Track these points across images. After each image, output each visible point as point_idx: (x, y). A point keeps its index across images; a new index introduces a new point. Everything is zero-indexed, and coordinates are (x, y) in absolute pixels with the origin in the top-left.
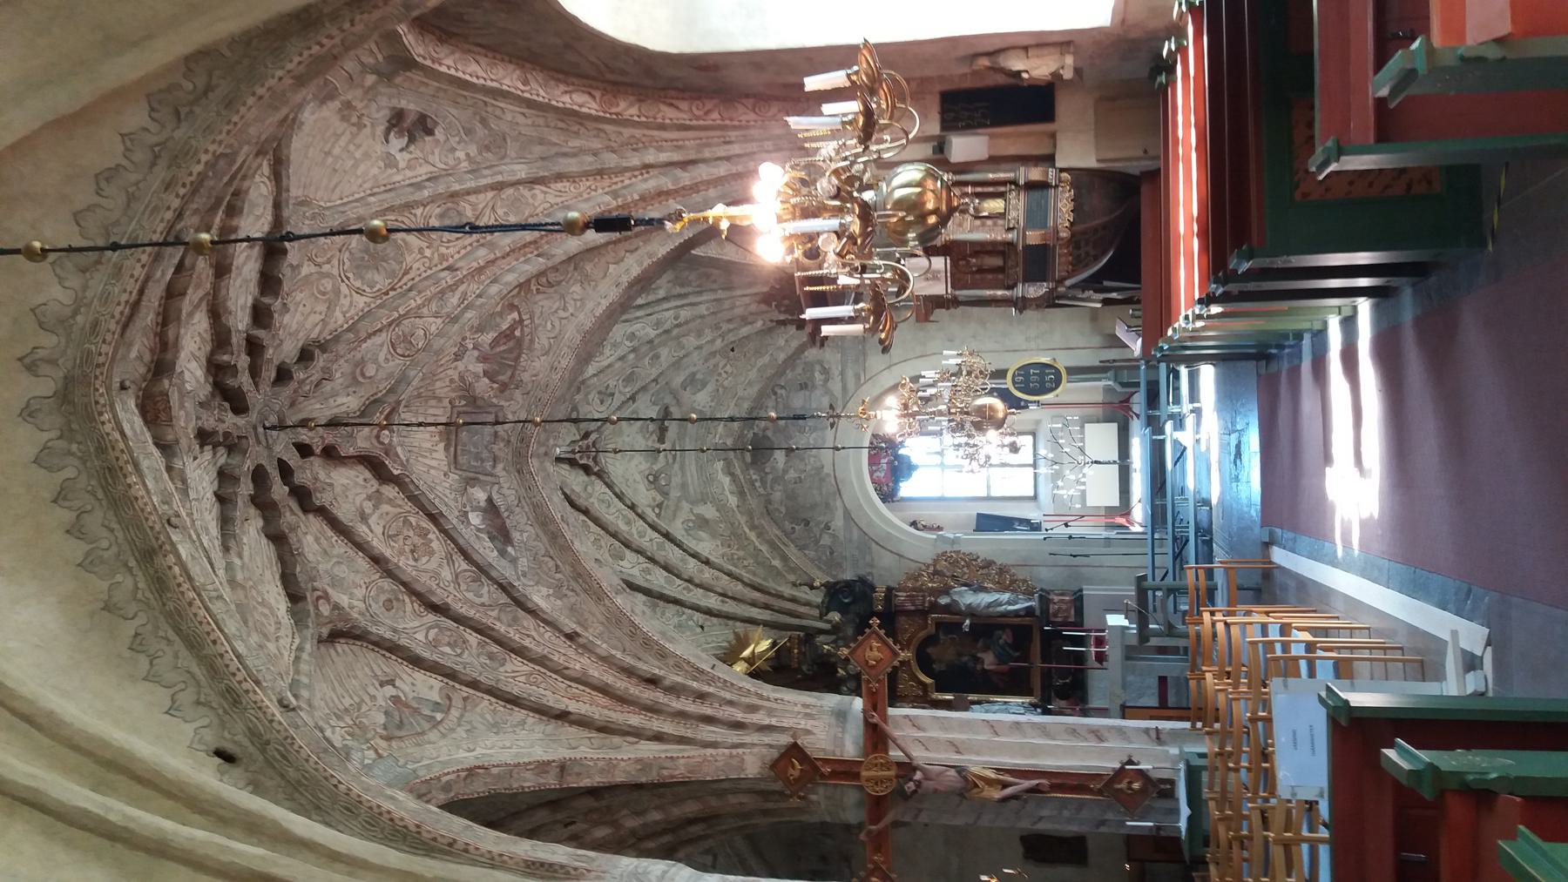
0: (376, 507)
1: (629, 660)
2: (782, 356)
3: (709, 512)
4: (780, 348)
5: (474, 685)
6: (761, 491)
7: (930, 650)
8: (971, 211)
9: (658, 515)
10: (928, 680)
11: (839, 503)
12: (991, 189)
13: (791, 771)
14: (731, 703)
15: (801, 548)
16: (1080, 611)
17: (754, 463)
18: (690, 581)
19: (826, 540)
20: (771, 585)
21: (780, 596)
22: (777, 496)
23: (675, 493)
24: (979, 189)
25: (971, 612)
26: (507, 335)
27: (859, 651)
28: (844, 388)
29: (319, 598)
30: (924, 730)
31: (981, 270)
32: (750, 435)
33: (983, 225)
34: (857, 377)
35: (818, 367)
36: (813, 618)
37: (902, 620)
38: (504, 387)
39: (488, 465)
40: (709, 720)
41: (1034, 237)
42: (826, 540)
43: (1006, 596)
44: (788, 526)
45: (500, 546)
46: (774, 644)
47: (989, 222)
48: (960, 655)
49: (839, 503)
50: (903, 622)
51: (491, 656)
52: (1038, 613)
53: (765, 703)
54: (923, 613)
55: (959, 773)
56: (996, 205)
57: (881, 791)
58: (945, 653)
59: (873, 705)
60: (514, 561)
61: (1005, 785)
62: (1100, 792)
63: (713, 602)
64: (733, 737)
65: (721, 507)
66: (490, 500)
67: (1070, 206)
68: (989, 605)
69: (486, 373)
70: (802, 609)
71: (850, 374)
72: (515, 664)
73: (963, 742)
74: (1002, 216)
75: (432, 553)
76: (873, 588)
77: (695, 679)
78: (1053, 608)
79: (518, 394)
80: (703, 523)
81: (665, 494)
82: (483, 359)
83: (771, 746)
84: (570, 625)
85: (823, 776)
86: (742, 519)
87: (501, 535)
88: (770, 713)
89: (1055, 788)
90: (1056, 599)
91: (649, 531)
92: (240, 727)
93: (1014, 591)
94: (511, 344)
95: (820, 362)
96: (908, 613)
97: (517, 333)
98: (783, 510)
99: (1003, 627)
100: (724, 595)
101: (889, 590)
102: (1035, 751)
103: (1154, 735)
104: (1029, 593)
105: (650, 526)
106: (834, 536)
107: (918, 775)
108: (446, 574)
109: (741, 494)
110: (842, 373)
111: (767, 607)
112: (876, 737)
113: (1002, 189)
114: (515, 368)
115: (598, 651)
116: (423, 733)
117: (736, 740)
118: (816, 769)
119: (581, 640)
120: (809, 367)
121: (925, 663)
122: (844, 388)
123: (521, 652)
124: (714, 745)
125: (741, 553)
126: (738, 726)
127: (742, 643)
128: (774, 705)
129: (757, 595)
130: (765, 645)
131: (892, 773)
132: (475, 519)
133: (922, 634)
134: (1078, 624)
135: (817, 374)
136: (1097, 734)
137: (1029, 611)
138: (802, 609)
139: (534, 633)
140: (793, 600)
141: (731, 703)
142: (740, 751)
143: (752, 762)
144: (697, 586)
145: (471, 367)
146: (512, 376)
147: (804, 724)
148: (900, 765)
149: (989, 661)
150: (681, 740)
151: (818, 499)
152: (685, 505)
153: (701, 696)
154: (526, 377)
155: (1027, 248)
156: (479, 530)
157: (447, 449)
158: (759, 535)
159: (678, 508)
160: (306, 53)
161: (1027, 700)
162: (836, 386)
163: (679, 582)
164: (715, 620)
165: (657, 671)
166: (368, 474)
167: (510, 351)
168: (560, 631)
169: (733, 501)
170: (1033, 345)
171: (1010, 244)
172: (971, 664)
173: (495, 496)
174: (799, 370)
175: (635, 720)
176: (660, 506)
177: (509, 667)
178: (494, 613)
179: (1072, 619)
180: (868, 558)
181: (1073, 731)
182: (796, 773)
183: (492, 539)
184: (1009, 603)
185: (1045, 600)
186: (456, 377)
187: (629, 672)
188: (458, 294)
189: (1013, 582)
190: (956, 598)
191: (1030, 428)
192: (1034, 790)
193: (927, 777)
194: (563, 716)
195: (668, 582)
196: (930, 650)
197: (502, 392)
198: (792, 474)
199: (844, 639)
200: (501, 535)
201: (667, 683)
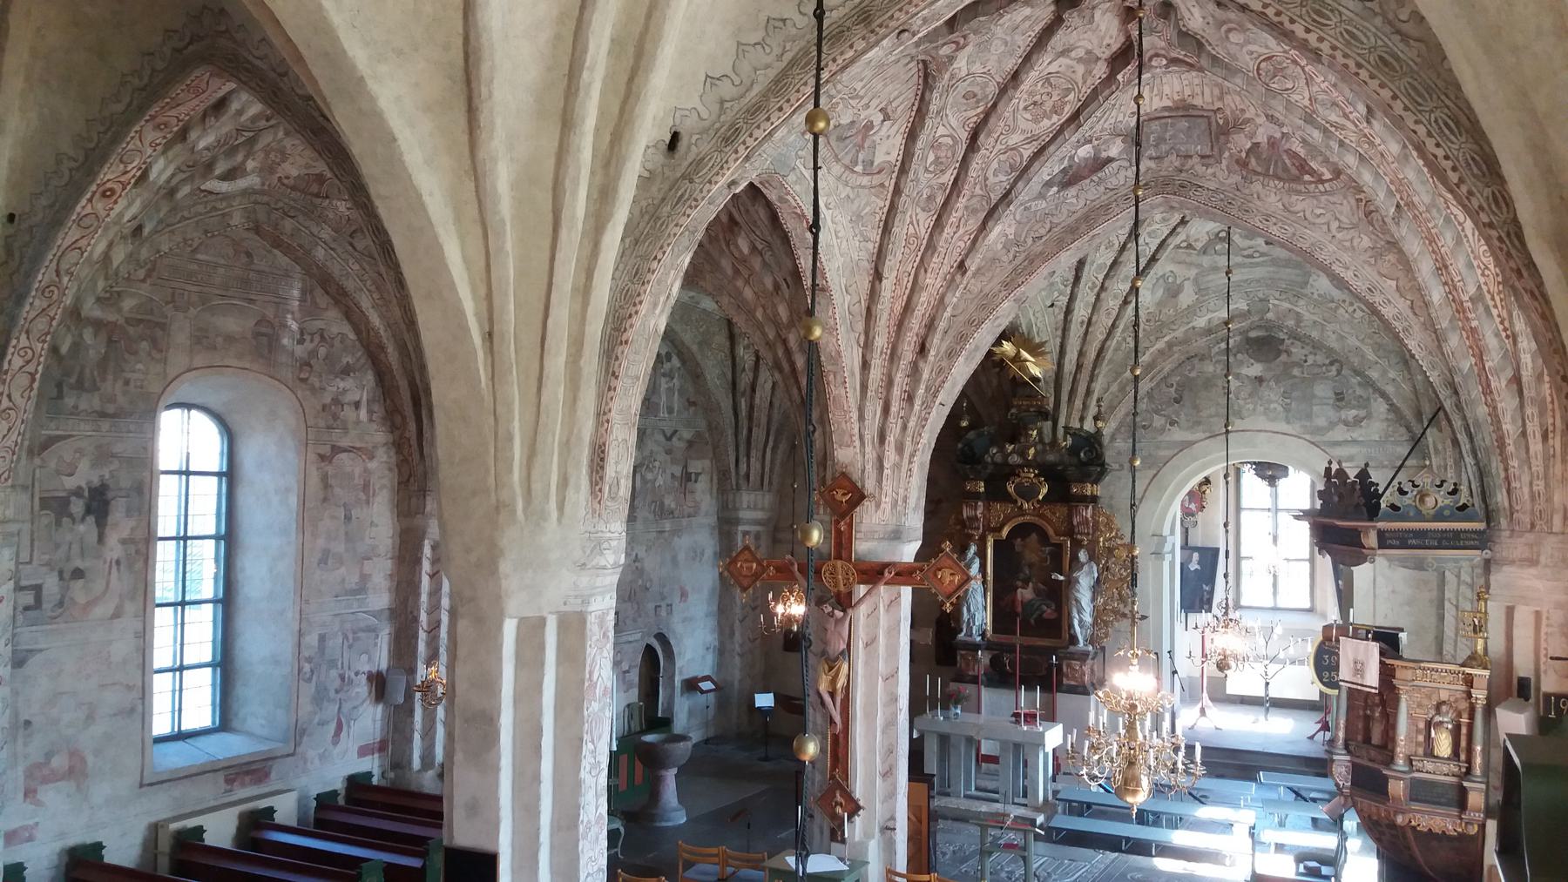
0: (1080, 60)
1: (942, 325)
2: (1374, 374)
3: (1187, 298)
4: (1385, 372)
5: (897, 191)
7: (1034, 536)
8: (1438, 719)
9: (1178, 247)
10: (1005, 532)
11: (1200, 435)
12: (1463, 744)
13: (841, 492)
14: (904, 428)
16: (1073, 690)
17: (1249, 341)
18: (1103, 288)
19: (1158, 421)
20: (1104, 368)
21: (1092, 379)
22: (1209, 368)
23: (1206, 261)
24: (1464, 730)
25: (1071, 583)
26: (1303, 167)
27: (949, 562)
29: (957, 43)
30: (887, 611)
31: (1368, 719)
33: (1418, 731)
35: (1362, 413)
36: (1069, 416)
37: (1065, 510)
38: (1243, 164)
39: (1152, 152)
40: (886, 410)
41: (1397, 788)
42: (1158, 421)
43: (1088, 619)
44: (1175, 379)
45: (1057, 180)
46: (1036, 380)
47: (1421, 738)
48: (1031, 566)
50: (1061, 511)
51: (930, 198)
52: (1072, 648)
53: (906, 461)
54: (1070, 532)
55: (842, 653)
56: (1443, 745)
57: (826, 577)
58: (1031, 552)
59: (903, 574)
60: (1041, 196)
61: (832, 695)
62: (833, 777)
63: (1081, 312)
64: (871, 433)
65: (1191, 311)
66: (1110, 160)
67: (1437, 830)
68: (1077, 601)
69: (1256, 145)
70: (1078, 403)
72: (925, 221)
73: (876, 650)
74: (1430, 753)
75: (1036, 120)
76: (1096, 482)
77: (928, 389)
78: (1076, 664)
79: (1236, 178)
80: (1174, 292)
81: (1204, 251)
82: (1273, 143)
83: (863, 471)
84: (972, 265)
85: (837, 522)
86: (1179, 333)
87: (1070, 178)
88: (897, 466)
89: (835, 738)
90: (1086, 669)
91: (1158, 241)
92: (705, 147)
93: (1095, 623)
94: (1294, 171)
95: (1369, 416)
96: (1070, 517)
97: (1307, 178)
98: (1193, 375)
99: (1059, 610)
100: (1089, 323)
101: (1094, 499)
102: (870, 716)
103: (890, 824)
104: (1091, 640)
105: (1164, 241)
106: (1162, 430)
107: (839, 614)
108: (1015, 139)
109: (1208, 331)
110: (1354, 441)
111: (1079, 366)
112: (874, 573)
113: (1463, 757)
114: (1266, 175)
115: (949, 295)
116: (838, 160)
117: (868, 438)
118: (843, 516)
119: (958, 277)
120: (1364, 403)
121: (1021, 531)
123: (938, 225)
124: (861, 418)
126: (882, 438)
127: (1036, 350)
128: (904, 470)
129: (1092, 355)
130: (1036, 371)
131: (842, 588)
132: (1085, 152)
133: (1051, 532)
134: (1060, 688)
135: (1354, 412)
136: (889, 773)
137: (1073, 640)
138: (1078, 403)
139: (961, 231)
140: (1089, 392)
141: (904, 428)
142: (857, 443)
143: (851, 454)
144: (1098, 296)
145: (1261, 130)
146: (1256, 173)
147: (886, 501)
148: (850, 594)
149: (1025, 594)
150: (864, 387)
151: (1204, 414)
152: (1193, 272)
153: (910, 399)
154: (1257, 187)
155: (1386, 779)
156: (1072, 158)
157: (1166, 108)
158: (1161, 352)
159: (1191, 264)
160: (1448, 164)
161: (989, 628)
162: (1340, 433)
163: (1101, 277)
164: (1062, 317)
165: (932, 353)
166: (1115, 47)
167: (1286, 169)
168: (967, 256)
169: (1201, 322)
171: (1390, 760)
172: (1022, 576)
173: (1115, 165)
174: (1359, 391)
175: (881, 341)
176: (1190, 246)
177: (922, 216)
178: (978, 191)
179: (1065, 681)
181: (891, 751)
182: (839, 497)
183: (1064, 171)
184: (1081, 621)
185: (1083, 656)
186: (1247, 115)
187: (930, 326)
188: (1342, 121)
189: (1106, 623)
190: (1086, 568)
191: (1318, 607)
192: (832, 721)
193: (839, 622)
194: (878, 276)
195: (1100, 267)
196: (1034, 536)
197: (1237, 162)
199: (1044, 451)
200: (1070, 178)
201: (921, 364)
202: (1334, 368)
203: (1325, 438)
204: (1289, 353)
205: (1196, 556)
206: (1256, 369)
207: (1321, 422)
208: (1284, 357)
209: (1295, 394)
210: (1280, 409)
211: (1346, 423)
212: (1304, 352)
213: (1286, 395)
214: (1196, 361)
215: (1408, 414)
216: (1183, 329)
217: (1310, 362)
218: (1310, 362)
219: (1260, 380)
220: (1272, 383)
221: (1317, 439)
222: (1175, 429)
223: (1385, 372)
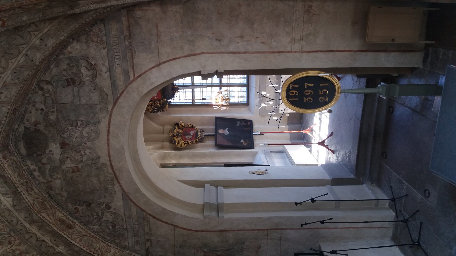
2: (38, 57)
4: (34, 47)
6: (41, 179)
11: (117, 188)
15: (86, 224)
17: (29, 155)
19: (108, 217)
28: (114, 85)
32: (22, 129)
34: (126, 74)
35: (83, 63)
42: (108, 217)
49: (117, 188)
71: (118, 70)
86: (21, 217)
95: (85, 58)
98: (65, 194)
110: (110, 70)
122: (114, 85)
125: (23, 248)
135: (83, 70)
162: (104, 81)
170: (297, 47)
174: (64, 66)
180: (147, 229)
198: (69, 165)
202: (46, 87)
203: (109, 93)
204: (36, 123)
205: (220, 131)
206: (55, 149)
207: (95, 97)
208: (41, 127)
209: (73, 117)
210: (87, 129)
211: (94, 76)
212: (34, 111)
213: (74, 124)
214: (52, 193)
215: (74, 26)
216: (17, 214)
217: (42, 106)
218: (42, 106)
219: (63, 145)
220: (65, 135)
221: (110, 99)
222: (113, 205)
223: (34, 47)
